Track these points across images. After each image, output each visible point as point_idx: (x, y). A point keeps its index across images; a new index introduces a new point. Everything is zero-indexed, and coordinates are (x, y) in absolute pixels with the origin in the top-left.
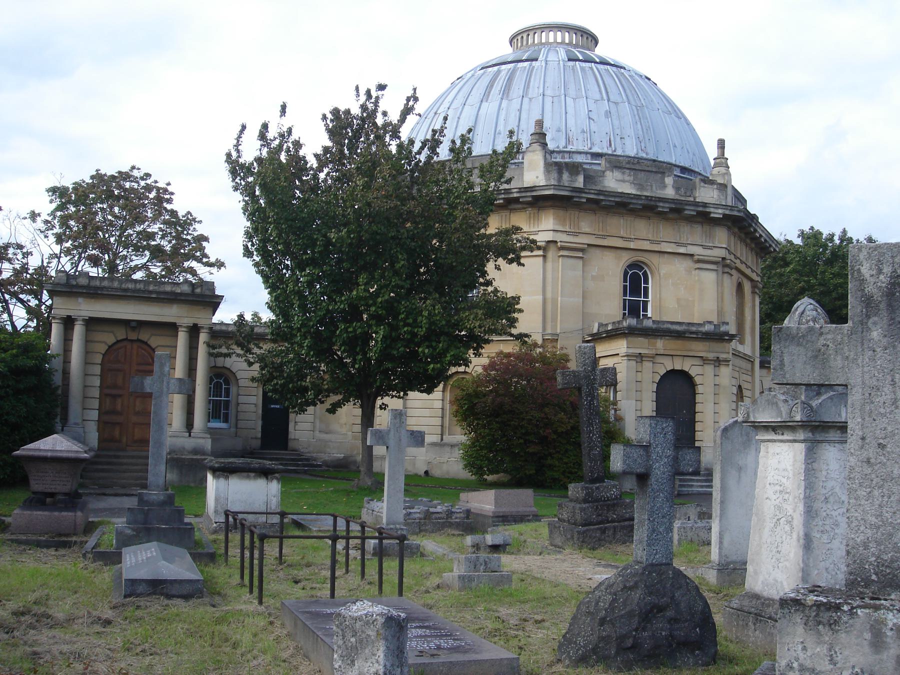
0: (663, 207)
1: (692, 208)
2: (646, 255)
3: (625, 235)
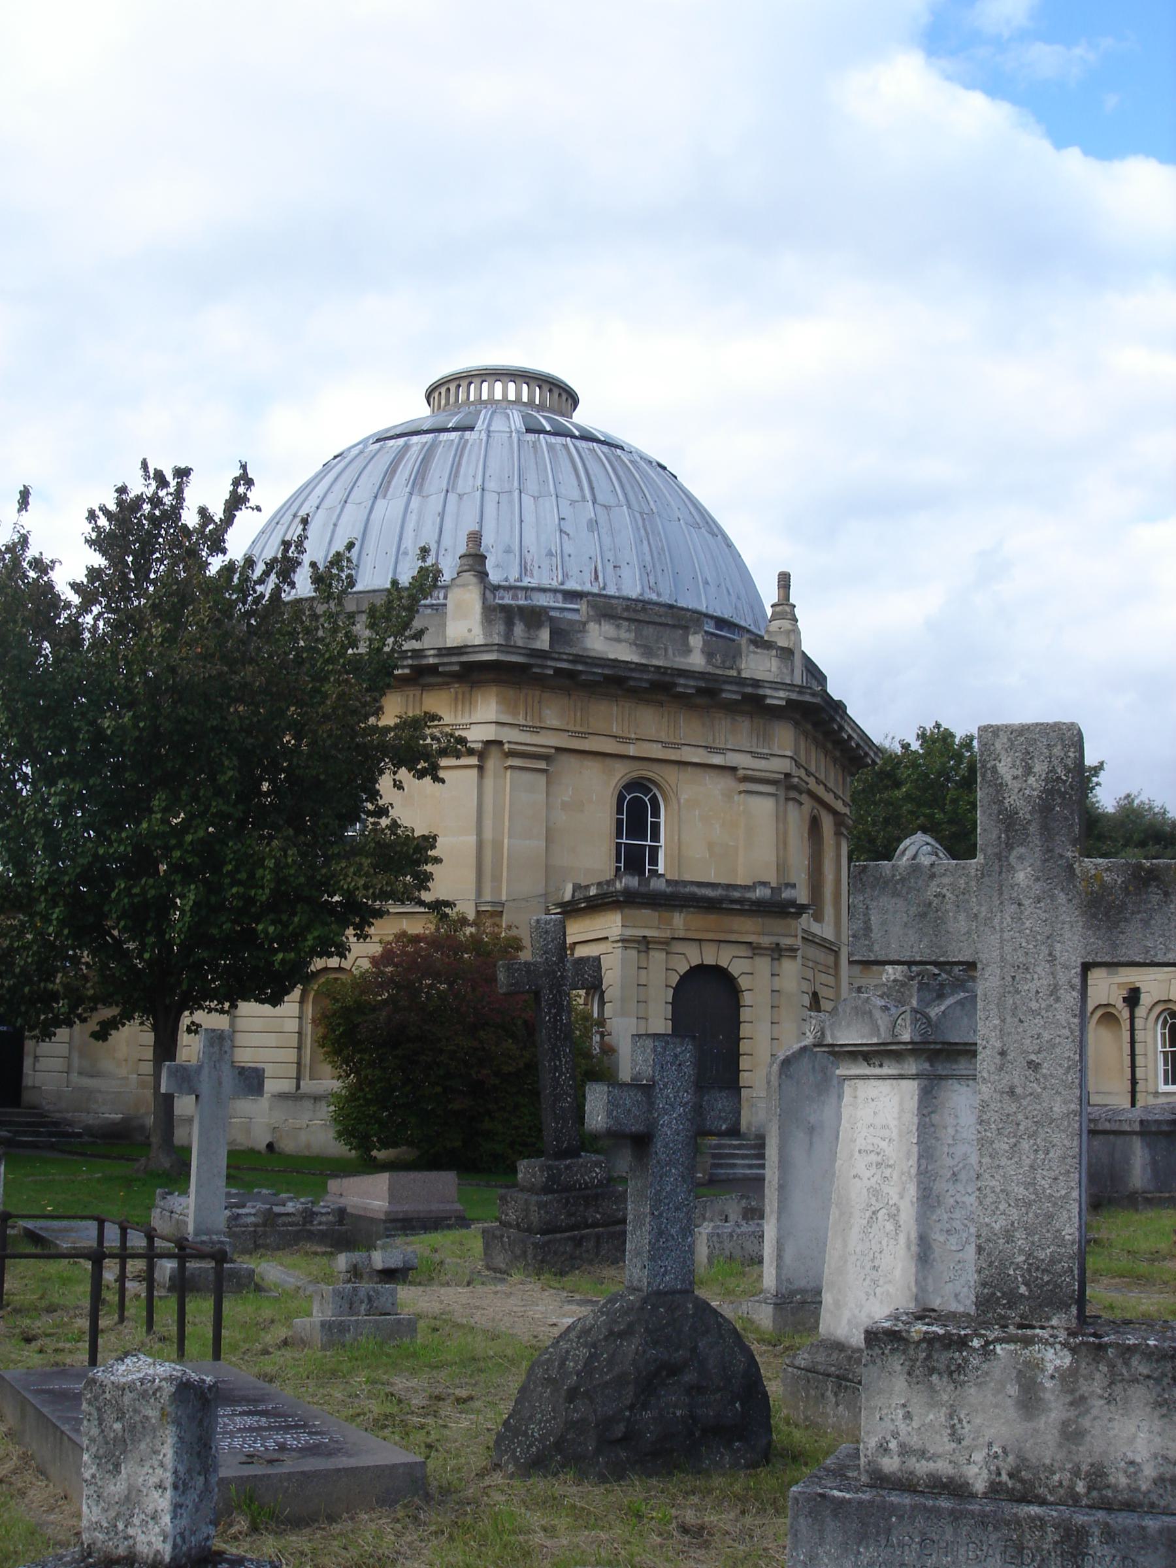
0: (686, 686)
1: (734, 688)
2: (656, 767)
3: (620, 733)
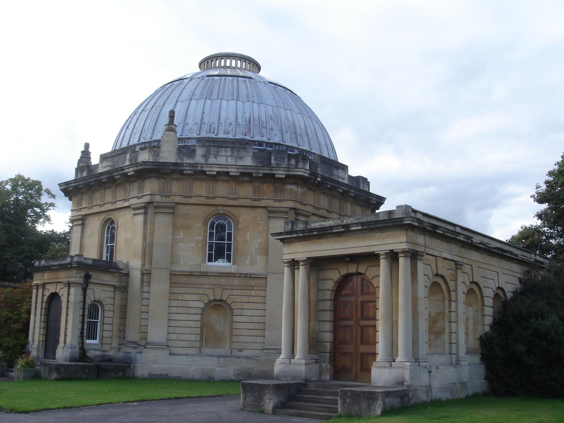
0: (104, 179)
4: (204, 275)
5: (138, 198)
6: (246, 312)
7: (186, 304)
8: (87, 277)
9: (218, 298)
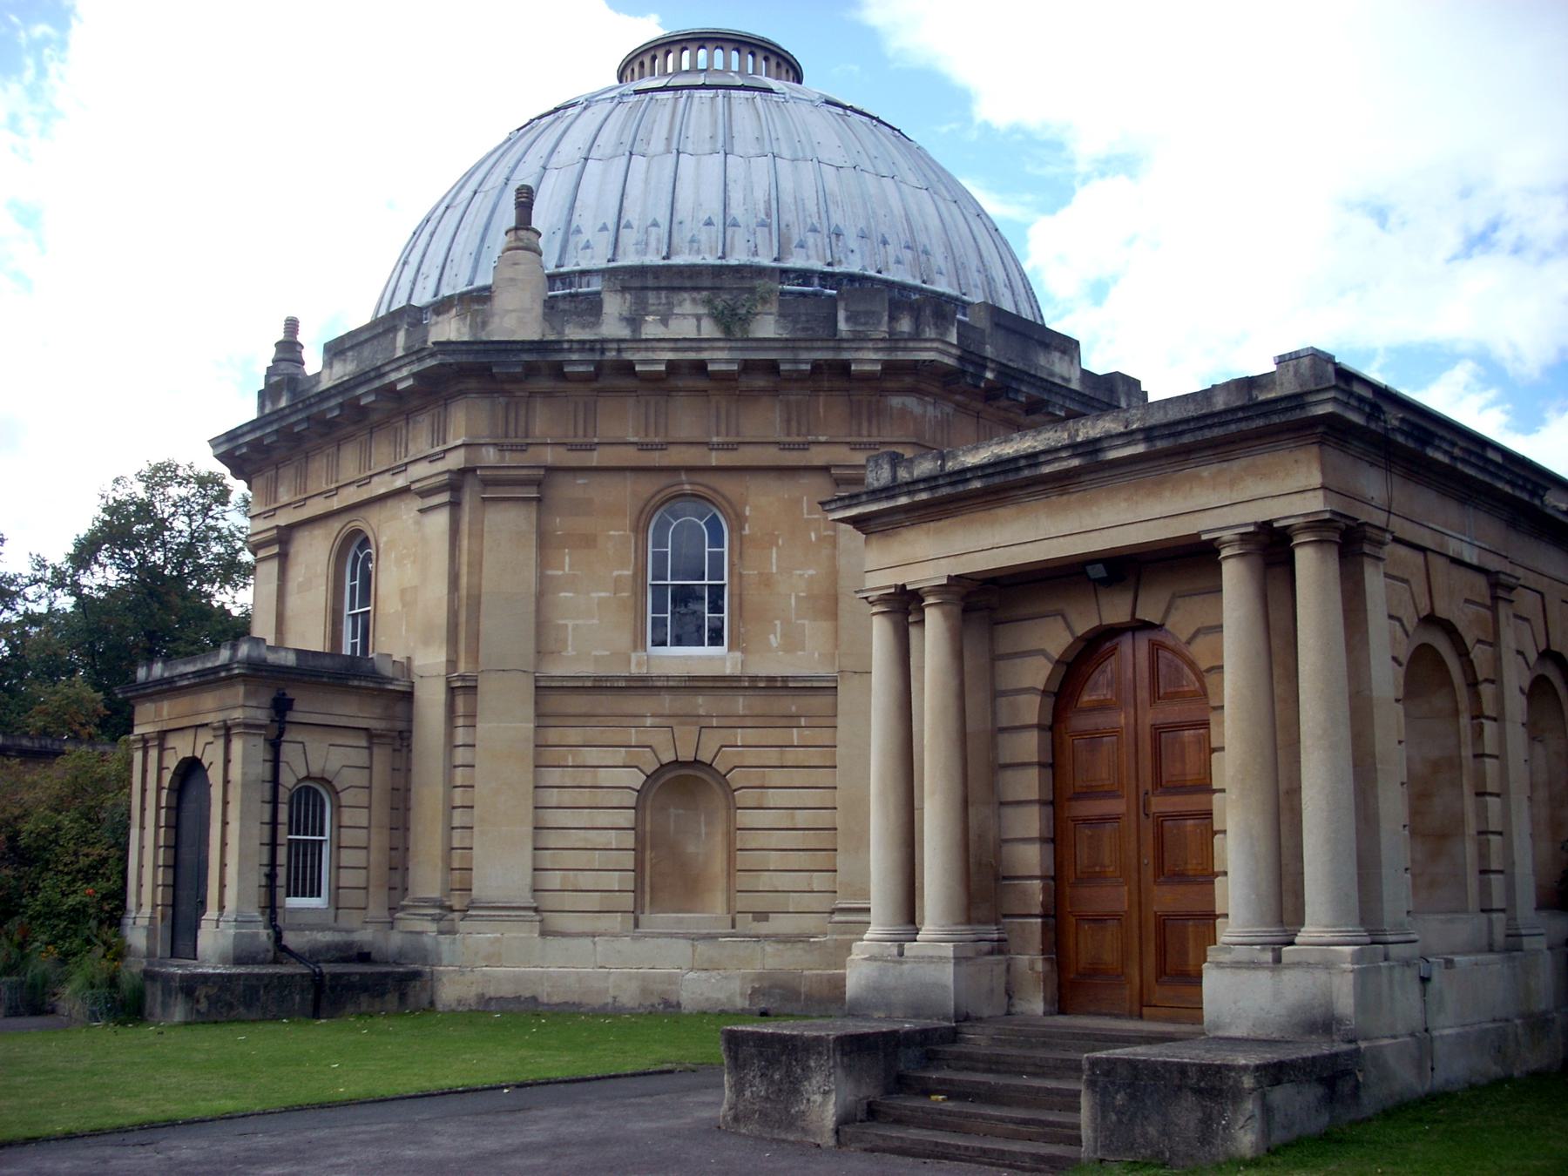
0: (331, 409)
4: (643, 686)
5: (431, 459)
6: (774, 798)
7: (587, 777)
8: (281, 706)
9: (686, 755)
